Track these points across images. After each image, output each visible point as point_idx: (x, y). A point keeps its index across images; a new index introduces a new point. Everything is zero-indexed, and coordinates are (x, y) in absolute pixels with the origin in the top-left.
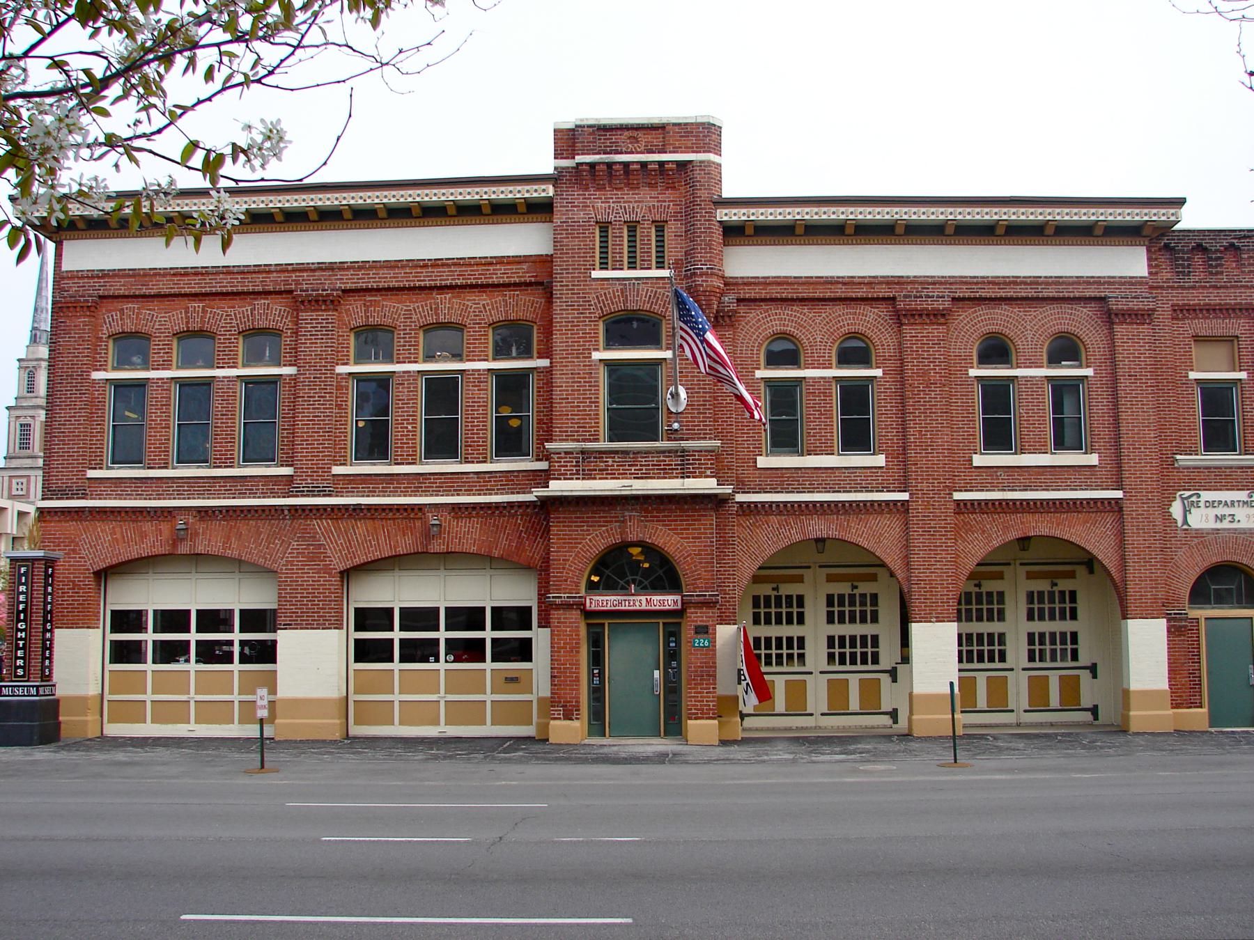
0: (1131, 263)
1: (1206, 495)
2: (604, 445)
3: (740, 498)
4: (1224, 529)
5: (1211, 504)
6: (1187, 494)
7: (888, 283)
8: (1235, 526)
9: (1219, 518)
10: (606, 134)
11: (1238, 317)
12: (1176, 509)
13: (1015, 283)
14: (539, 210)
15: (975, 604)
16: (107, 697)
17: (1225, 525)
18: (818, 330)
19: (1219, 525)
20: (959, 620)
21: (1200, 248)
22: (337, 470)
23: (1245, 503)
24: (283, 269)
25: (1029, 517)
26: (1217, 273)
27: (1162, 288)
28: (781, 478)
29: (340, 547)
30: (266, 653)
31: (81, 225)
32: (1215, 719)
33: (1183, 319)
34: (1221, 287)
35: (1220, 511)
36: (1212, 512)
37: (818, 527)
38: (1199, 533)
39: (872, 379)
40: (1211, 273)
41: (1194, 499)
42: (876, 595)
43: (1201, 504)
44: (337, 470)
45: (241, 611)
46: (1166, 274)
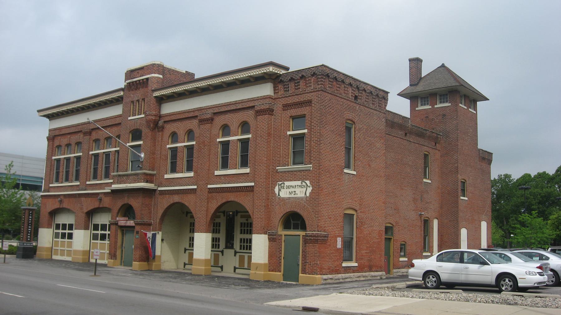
0: (266, 90)
1: (287, 183)
2: (130, 172)
3: (159, 189)
4: (292, 198)
5: (288, 187)
6: (281, 183)
7: (198, 110)
8: (296, 196)
9: (290, 193)
10: (132, 71)
11: (306, 106)
12: (276, 190)
13: (230, 105)
14: (117, 101)
15: (214, 228)
16: (54, 248)
17: (293, 196)
18: (234, 120)
19: (290, 196)
20: (213, 232)
21: (302, 77)
22: (88, 183)
23: (300, 186)
24: (78, 125)
25: (229, 194)
26: (298, 89)
27: (279, 98)
28: (171, 182)
29: (90, 205)
30: (70, 236)
31: (187, 93)
32: (285, 278)
33: (287, 110)
34: (299, 94)
35: (293, 190)
36: (288, 190)
37: (176, 199)
38: (283, 199)
39: (249, 138)
40: (296, 89)
41: (283, 185)
42: (220, 223)
43: (285, 187)
44: (88, 183)
45: (69, 224)
46: (281, 92)
